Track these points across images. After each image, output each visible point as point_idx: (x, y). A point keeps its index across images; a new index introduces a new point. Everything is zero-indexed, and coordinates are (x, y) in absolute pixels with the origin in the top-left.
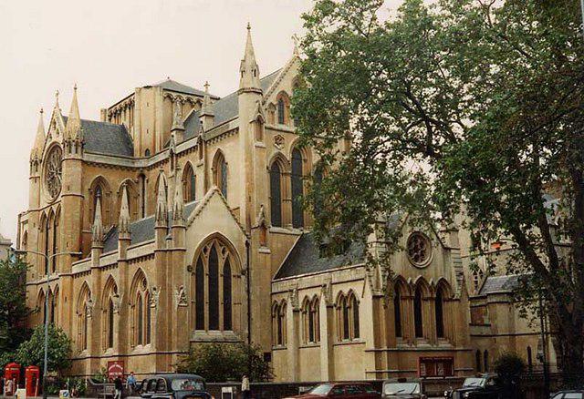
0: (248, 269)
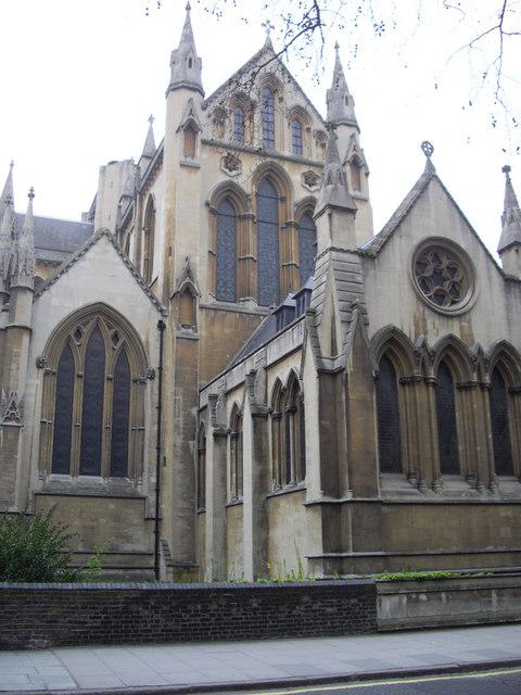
0: (160, 369)
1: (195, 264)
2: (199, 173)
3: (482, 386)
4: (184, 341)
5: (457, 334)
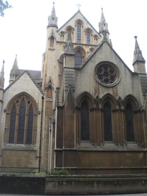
1: (53, 79)
2: (54, 51)
3: (121, 110)
4: (48, 102)
5: (111, 93)
